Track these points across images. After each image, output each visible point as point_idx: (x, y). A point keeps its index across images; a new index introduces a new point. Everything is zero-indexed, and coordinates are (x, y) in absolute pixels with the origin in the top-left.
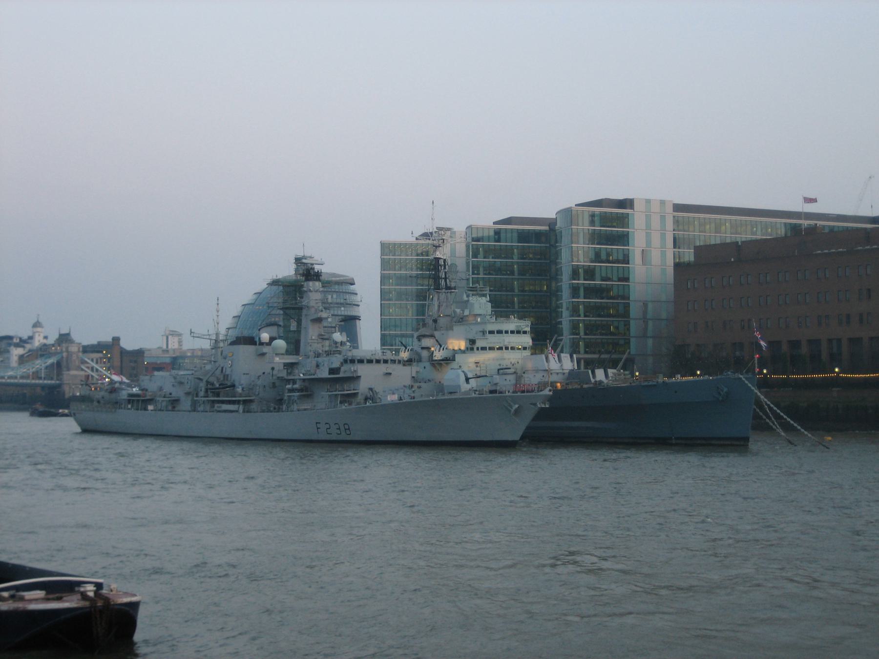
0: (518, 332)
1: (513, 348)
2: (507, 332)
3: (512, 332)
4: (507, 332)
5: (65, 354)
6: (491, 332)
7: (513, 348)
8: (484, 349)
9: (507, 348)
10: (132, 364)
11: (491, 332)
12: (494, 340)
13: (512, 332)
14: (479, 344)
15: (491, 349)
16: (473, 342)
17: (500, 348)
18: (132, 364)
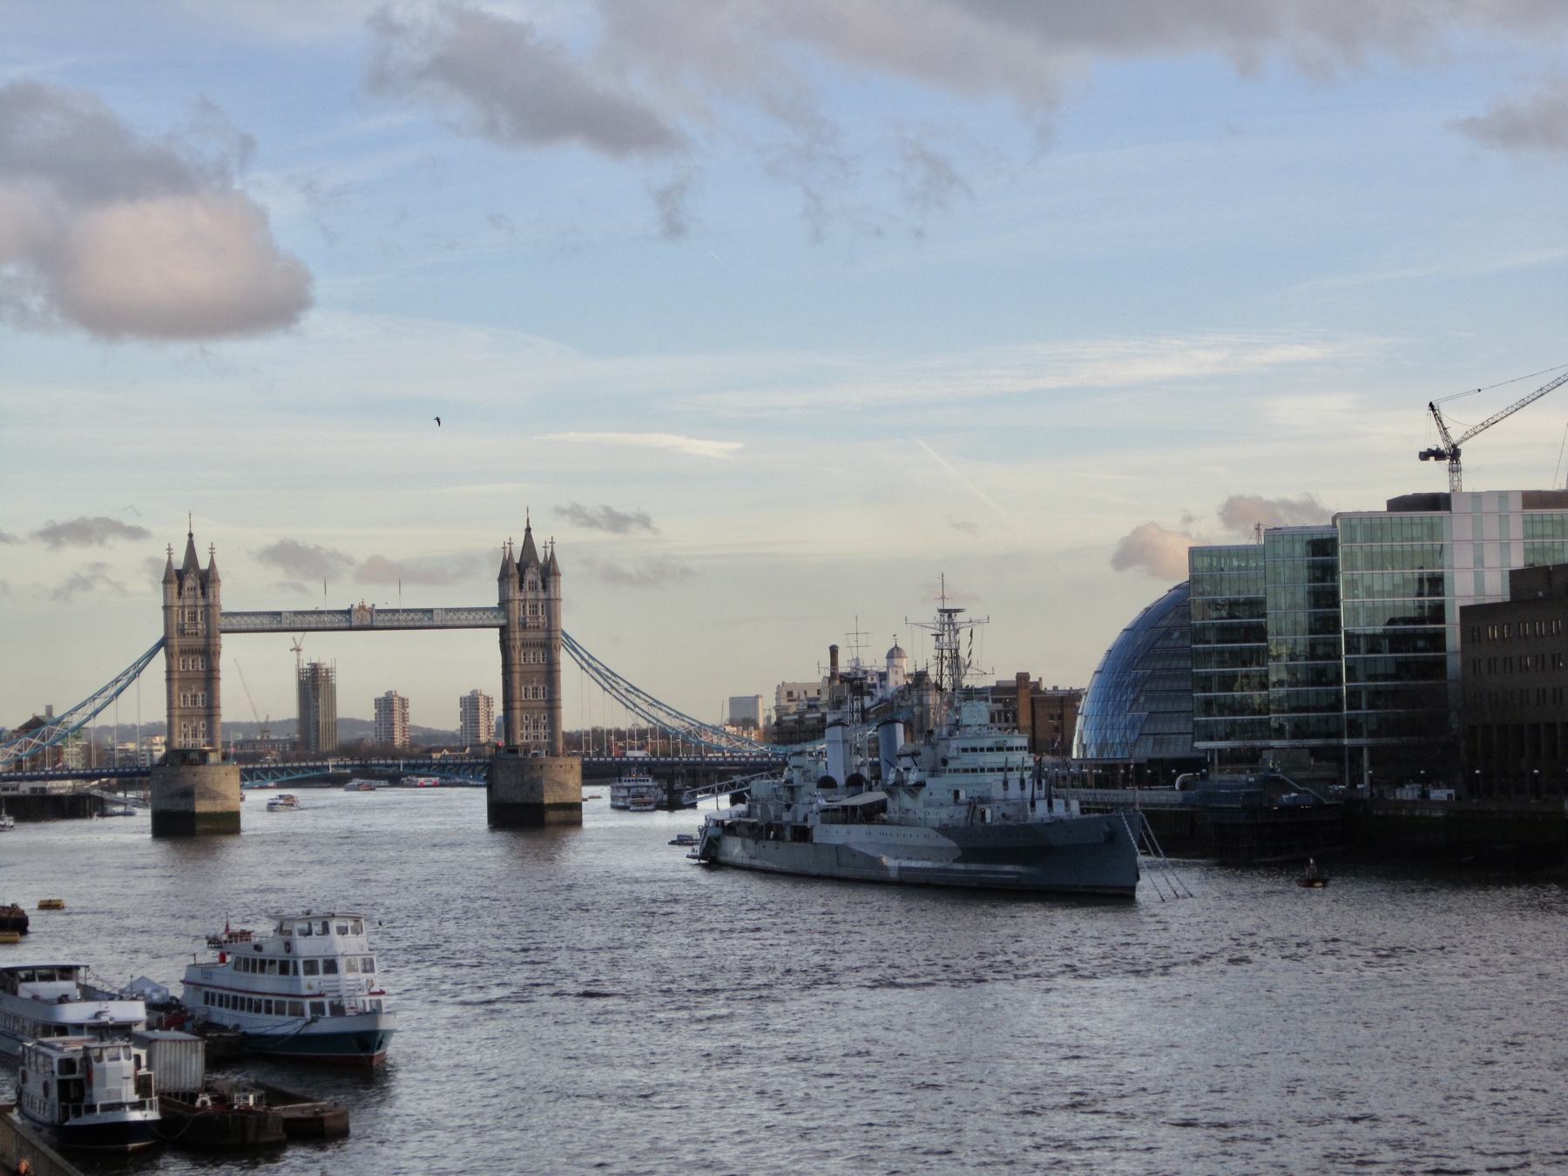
0: (1000, 749)
1: (991, 770)
2: (982, 750)
3: (990, 749)
4: (982, 750)
5: (916, 710)
6: (965, 750)
7: (991, 770)
8: (956, 771)
9: (982, 770)
10: (1055, 722)
11: (965, 750)
12: (968, 760)
13: (990, 749)
14: (952, 764)
15: (966, 771)
16: (945, 762)
17: (974, 770)
18: (1055, 722)
